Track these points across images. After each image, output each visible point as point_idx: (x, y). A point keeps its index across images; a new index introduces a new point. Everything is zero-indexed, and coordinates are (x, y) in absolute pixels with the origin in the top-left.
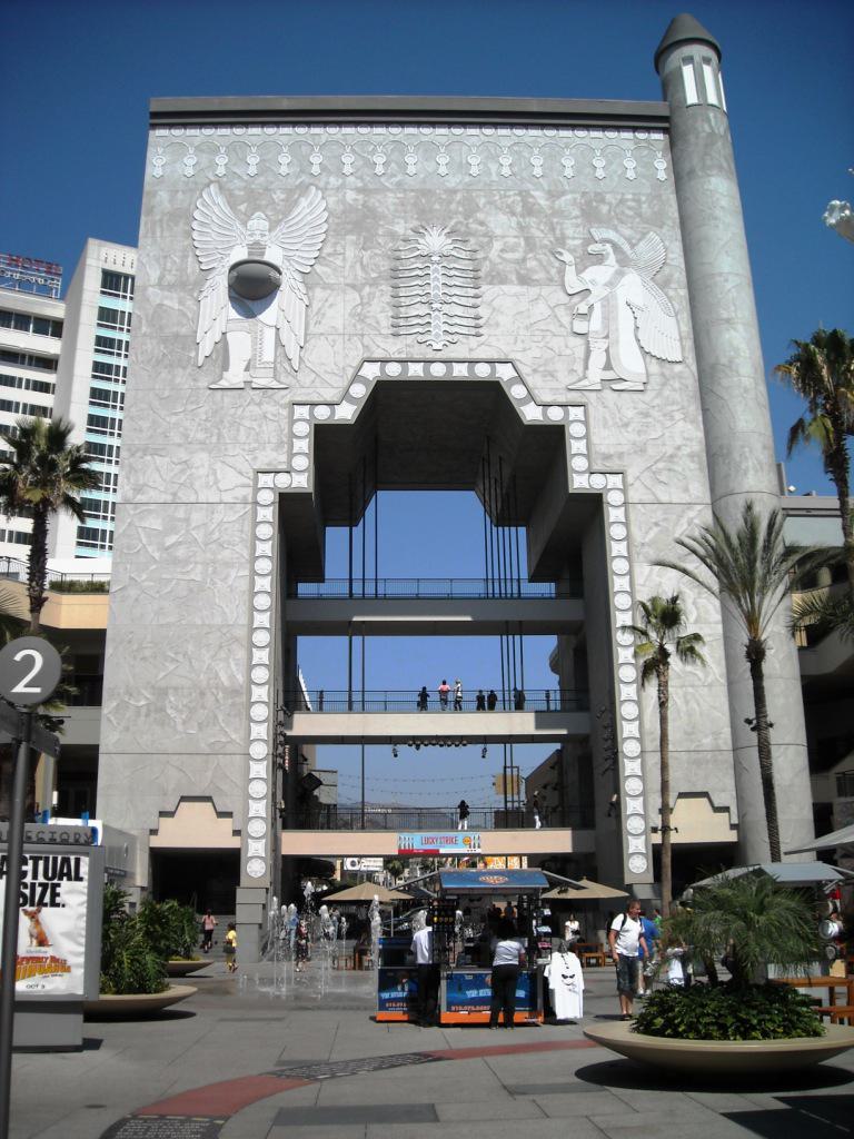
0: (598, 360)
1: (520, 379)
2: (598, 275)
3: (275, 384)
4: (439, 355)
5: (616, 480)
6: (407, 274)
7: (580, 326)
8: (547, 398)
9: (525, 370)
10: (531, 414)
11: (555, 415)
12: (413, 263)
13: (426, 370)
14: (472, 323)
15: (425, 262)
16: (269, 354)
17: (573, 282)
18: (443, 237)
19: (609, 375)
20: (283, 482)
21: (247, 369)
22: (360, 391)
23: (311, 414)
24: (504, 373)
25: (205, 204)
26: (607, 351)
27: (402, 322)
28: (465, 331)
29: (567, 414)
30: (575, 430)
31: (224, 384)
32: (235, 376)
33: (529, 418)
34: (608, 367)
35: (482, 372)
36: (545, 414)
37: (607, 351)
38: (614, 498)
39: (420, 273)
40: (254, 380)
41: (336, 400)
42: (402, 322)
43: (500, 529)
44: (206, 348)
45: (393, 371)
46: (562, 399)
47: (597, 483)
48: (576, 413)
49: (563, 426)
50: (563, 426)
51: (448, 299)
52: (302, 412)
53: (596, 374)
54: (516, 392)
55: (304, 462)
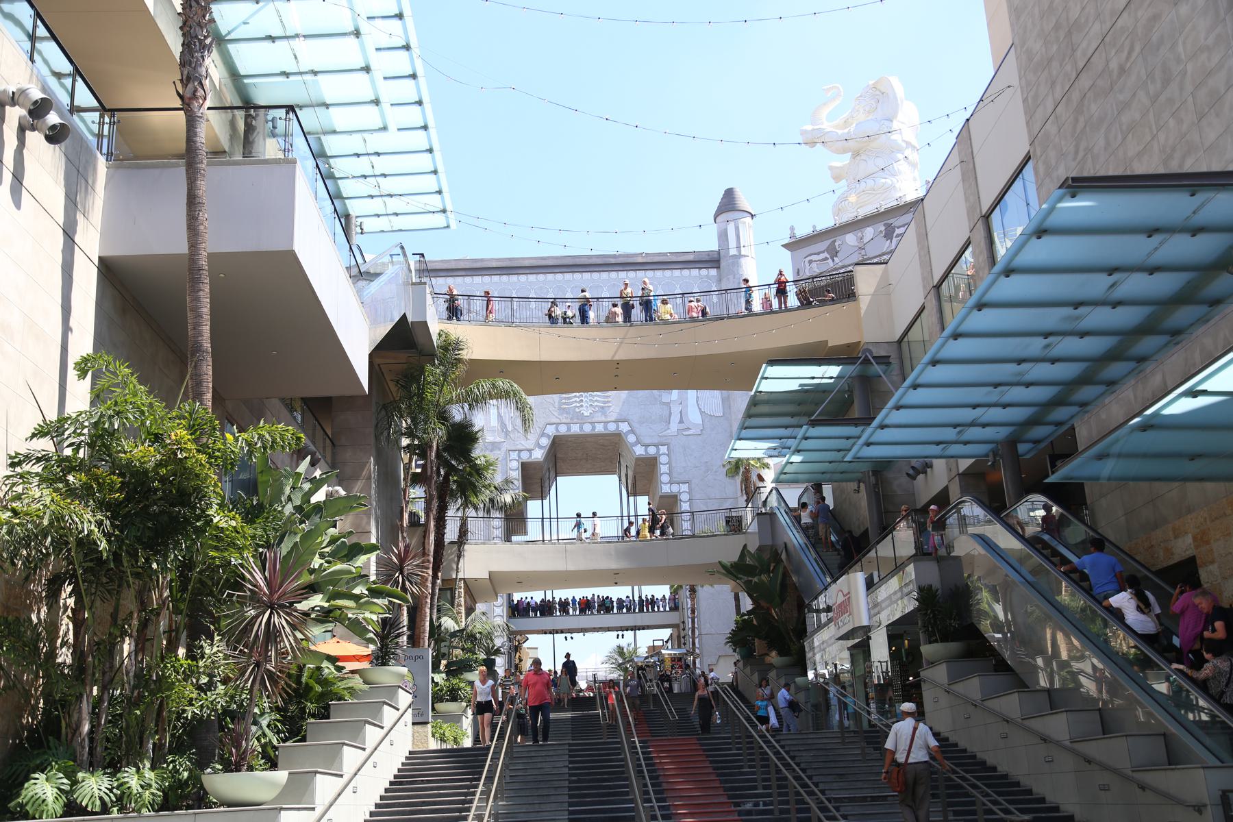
0: (675, 418)
5: (685, 487)
8: (647, 441)
9: (635, 425)
11: (652, 451)
13: (581, 428)
19: (682, 426)
22: (545, 442)
23: (519, 457)
29: (658, 450)
30: (663, 459)
34: (681, 422)
36: (646, 450)
37: (681, 412)
41: (532, 447)
43: (631, 499)
46: (656, 441)
47: (675, 488)
48: (663, 449)
52: (514, 455)
53: (674, 426)
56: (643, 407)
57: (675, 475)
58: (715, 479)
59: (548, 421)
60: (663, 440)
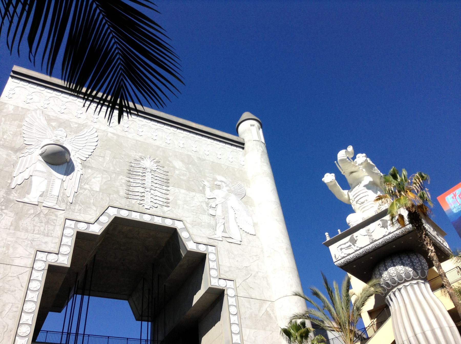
0: (220, 228)
1: (186, 229)
2: (219, 194)
3: (57, 207)
4: (148, 211)
5: (230, 284)
6: (135, 173)
7: (212, 212)
8: (199, 240)
9: (189, 226)
10: (191, 246)
11: (202, 249)
12: (138, 170)
14: (165, 201)
15: (144, 171)
16: (56, 192)
17: (208, 193)
18: (152, 163)
20: (53, 259)
21: (41, 196)
22: (106, 220)
24: (178, 225)
27: (130, 193)
28: (161, 203)
31: (25, 200)
32: (33, 197)
33: (190, 248)
34: (224, 231)
35: (168, 223)
36: (197, 247)
38: (229, 292)
39: (141, 174)
40: (45, 202)
41: (92, 221)
42: (130, 193)
44: (18, 180)
45: (124, 214)
46: (205, 242)
47: (221, 284)
48: (211, 249)
49: (206, 254)
50: (206, 254)
51: (153, 188)
53: (219, 234)
54: (183, 235)
56: (194, 214)
57: (222, 272)
58: (254, 282)
59: (111, 204)
60: (211, 242)
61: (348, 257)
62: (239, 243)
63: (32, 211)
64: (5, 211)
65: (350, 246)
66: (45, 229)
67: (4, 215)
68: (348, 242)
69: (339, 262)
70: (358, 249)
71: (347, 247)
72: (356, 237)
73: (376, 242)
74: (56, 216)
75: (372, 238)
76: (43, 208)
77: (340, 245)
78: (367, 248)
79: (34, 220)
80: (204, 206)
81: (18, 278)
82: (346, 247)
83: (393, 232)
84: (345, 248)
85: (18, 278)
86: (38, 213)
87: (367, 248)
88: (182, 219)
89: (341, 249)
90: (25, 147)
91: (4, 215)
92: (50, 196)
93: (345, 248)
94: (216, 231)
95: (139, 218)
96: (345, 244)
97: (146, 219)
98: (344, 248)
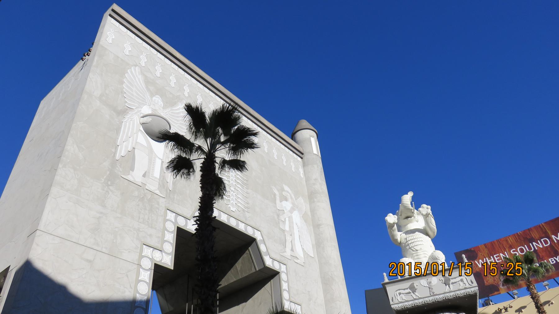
1: (264, 241)
3: (157, 192)
11: (276, 266)
21: (144, 176)
24: (257, 236)
25: (132, 72)
26: (291, 241)
32: (136, 176)
34: (292, 250)
35: (250, 232)
40: (147, 184)
55: (170, 248)
61: (406, 303)
62: (303, 264)
63: (136, 193)
64: (111, 188)
65: (409, 293)
66: (149, 219)
67: (110, 193)
68: (407, 289)
69: (396, 305)
70: (417, 298)
71: (406, 293)
72: (417, 285)
73: (437, 297)
74: (158, 204)
75: (433, 292)
76: (146, 191)
77: (399, 290)
78: (427, 299)
79: (138, 205)
80: (276, 217)
81: (127, 276)
82: (405, 293)
83: (454, 291)
84: (404, 294)
85: (127, 276)
86: (142, 197)
87: (427, 299)
88: (260, 229)
89: (400, 294)
90: (127, 110)
91: (110, 193)
92: (151, 178)
93: (404, 294)
94: (286, 247)
95: (227, 221)
96: (404, 289)
97: (233, 223)
98: (403, 294)
